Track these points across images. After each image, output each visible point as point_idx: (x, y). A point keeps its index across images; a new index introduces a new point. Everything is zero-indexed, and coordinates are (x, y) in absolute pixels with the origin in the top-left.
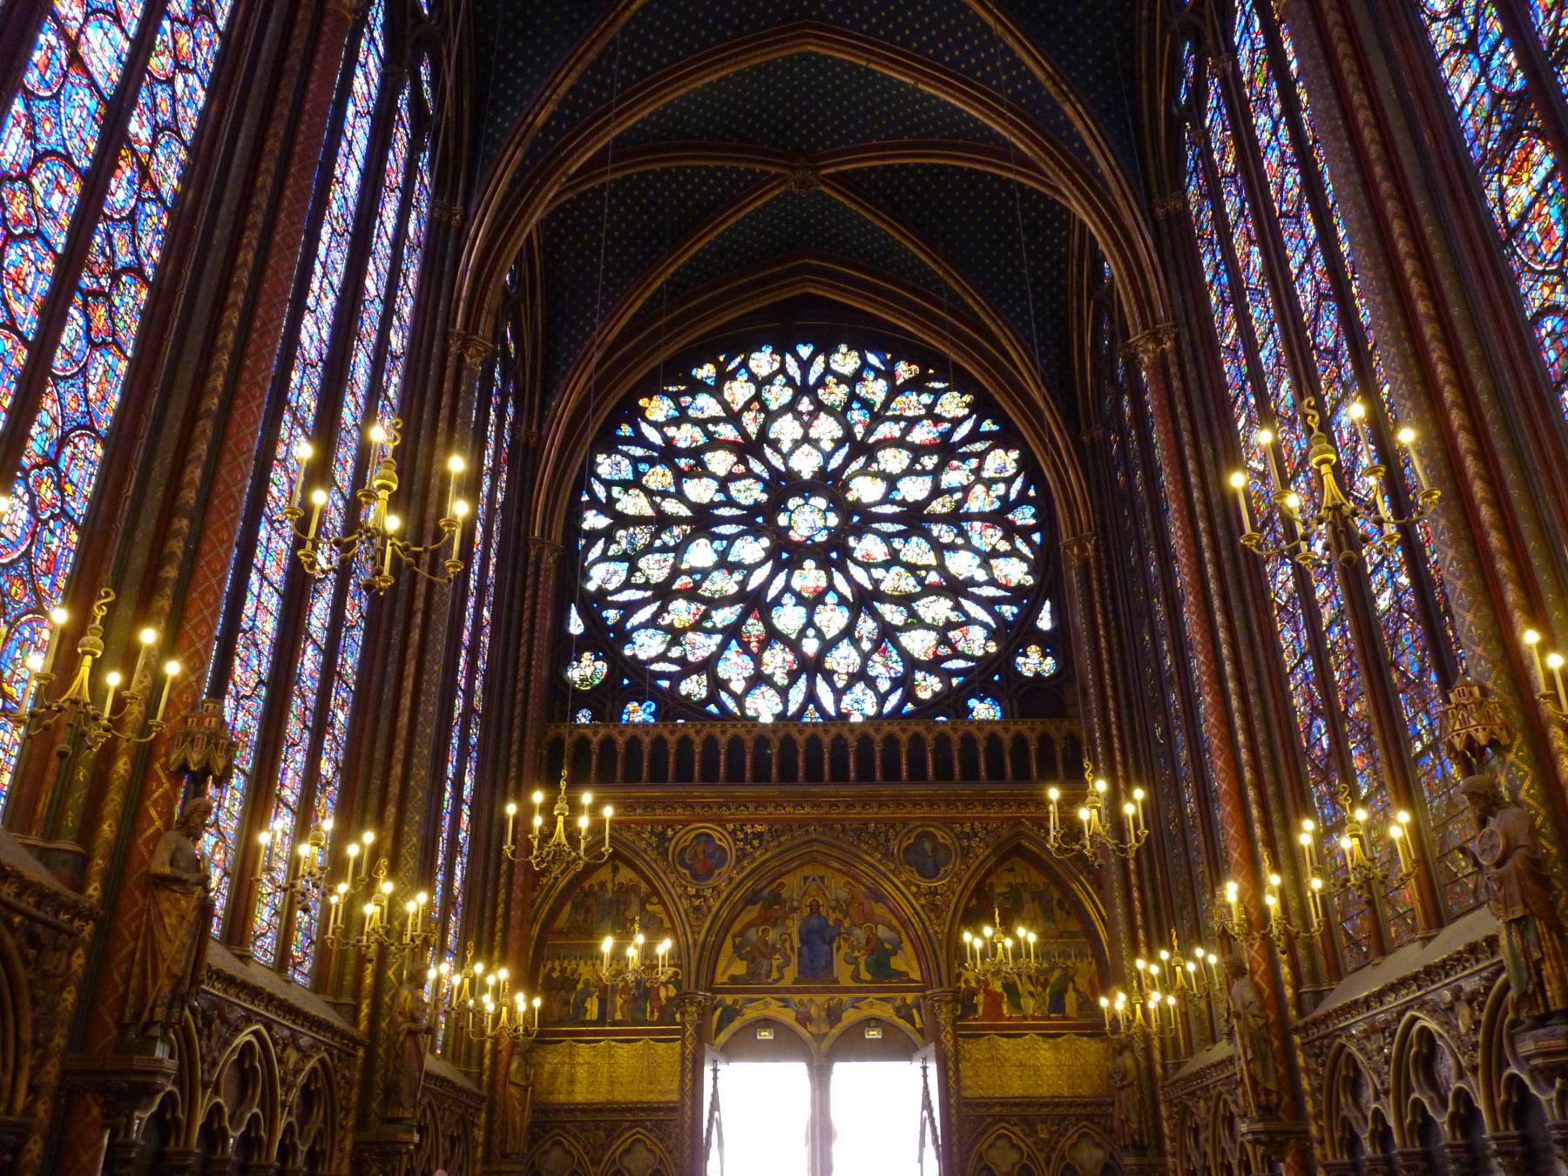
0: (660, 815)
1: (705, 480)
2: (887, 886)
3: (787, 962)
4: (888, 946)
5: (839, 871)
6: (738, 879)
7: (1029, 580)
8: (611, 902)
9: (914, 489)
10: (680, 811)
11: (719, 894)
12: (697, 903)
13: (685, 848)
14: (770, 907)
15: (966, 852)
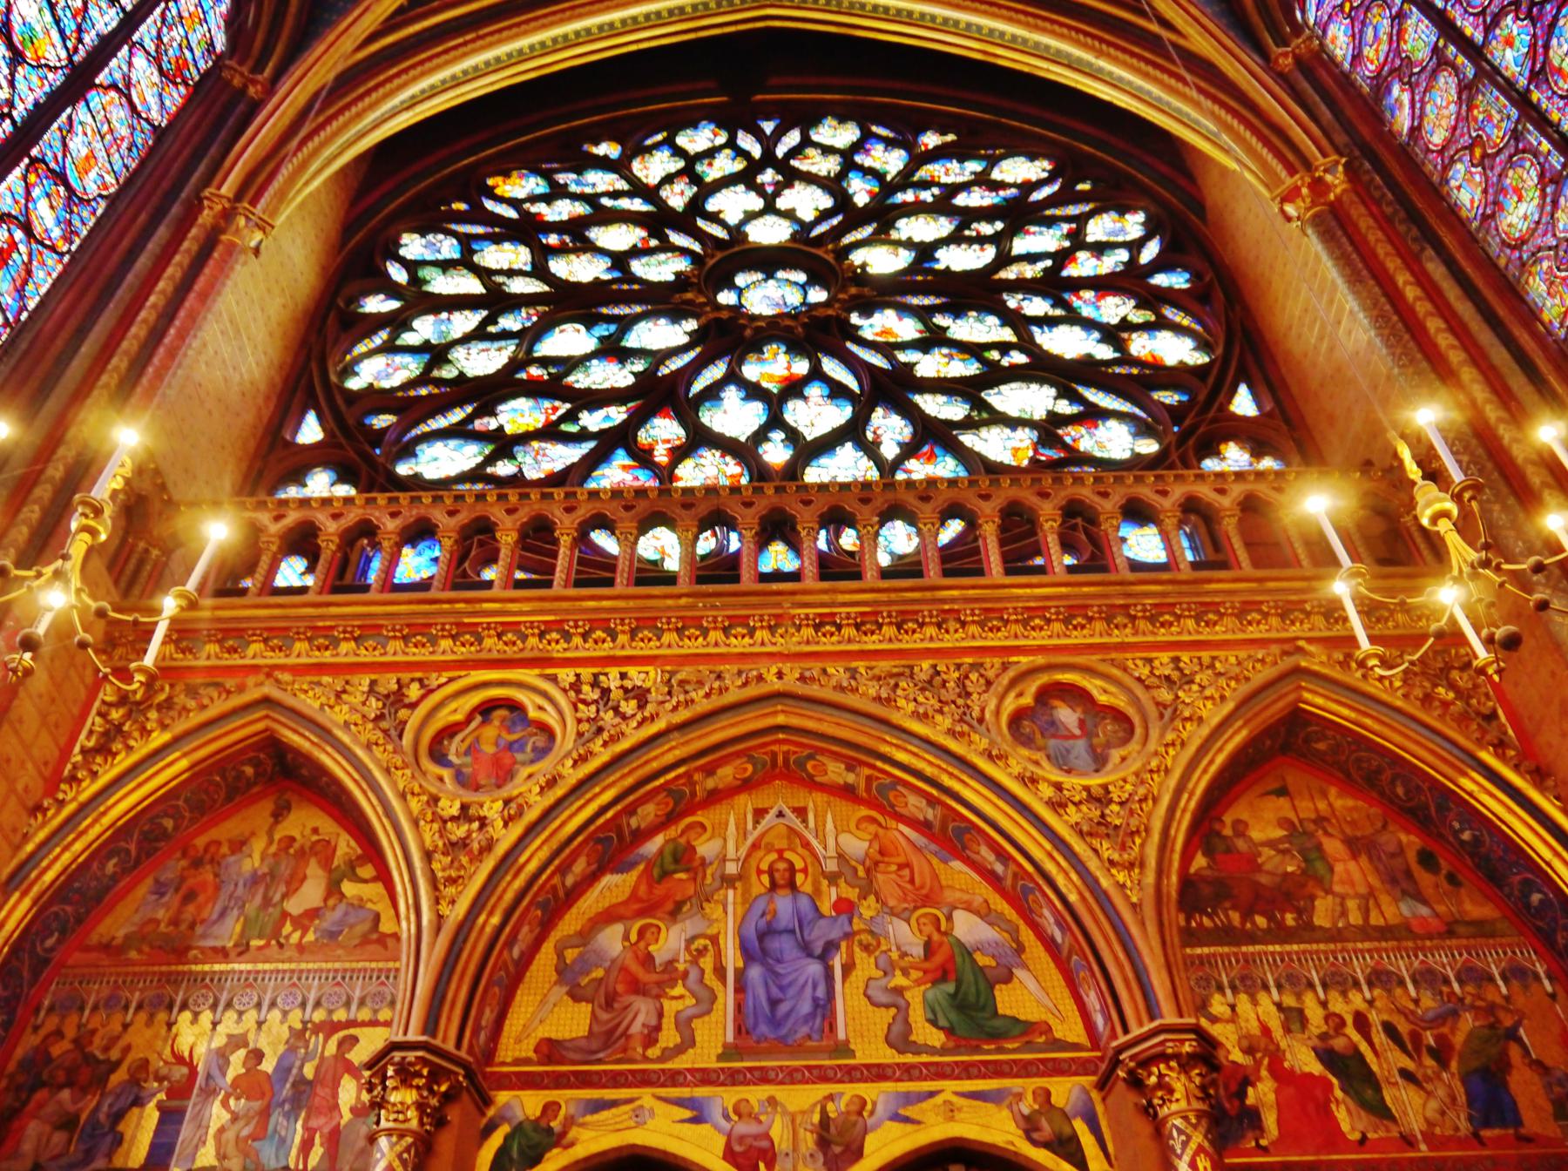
0: (395, 651)
1: (585, 257)
2: (973, 793)
3: (707, 1002)
4: (983, 960)
5: (846, 792)
6: (572, 776)
7: (1200, 359)
8: (255, 880)
9: (961, 259)
10: (445, 644)
11: (520, 813)
12: (459, 831)
13: (451, 731)
14: (666, 874)
15: (1171, 713)
